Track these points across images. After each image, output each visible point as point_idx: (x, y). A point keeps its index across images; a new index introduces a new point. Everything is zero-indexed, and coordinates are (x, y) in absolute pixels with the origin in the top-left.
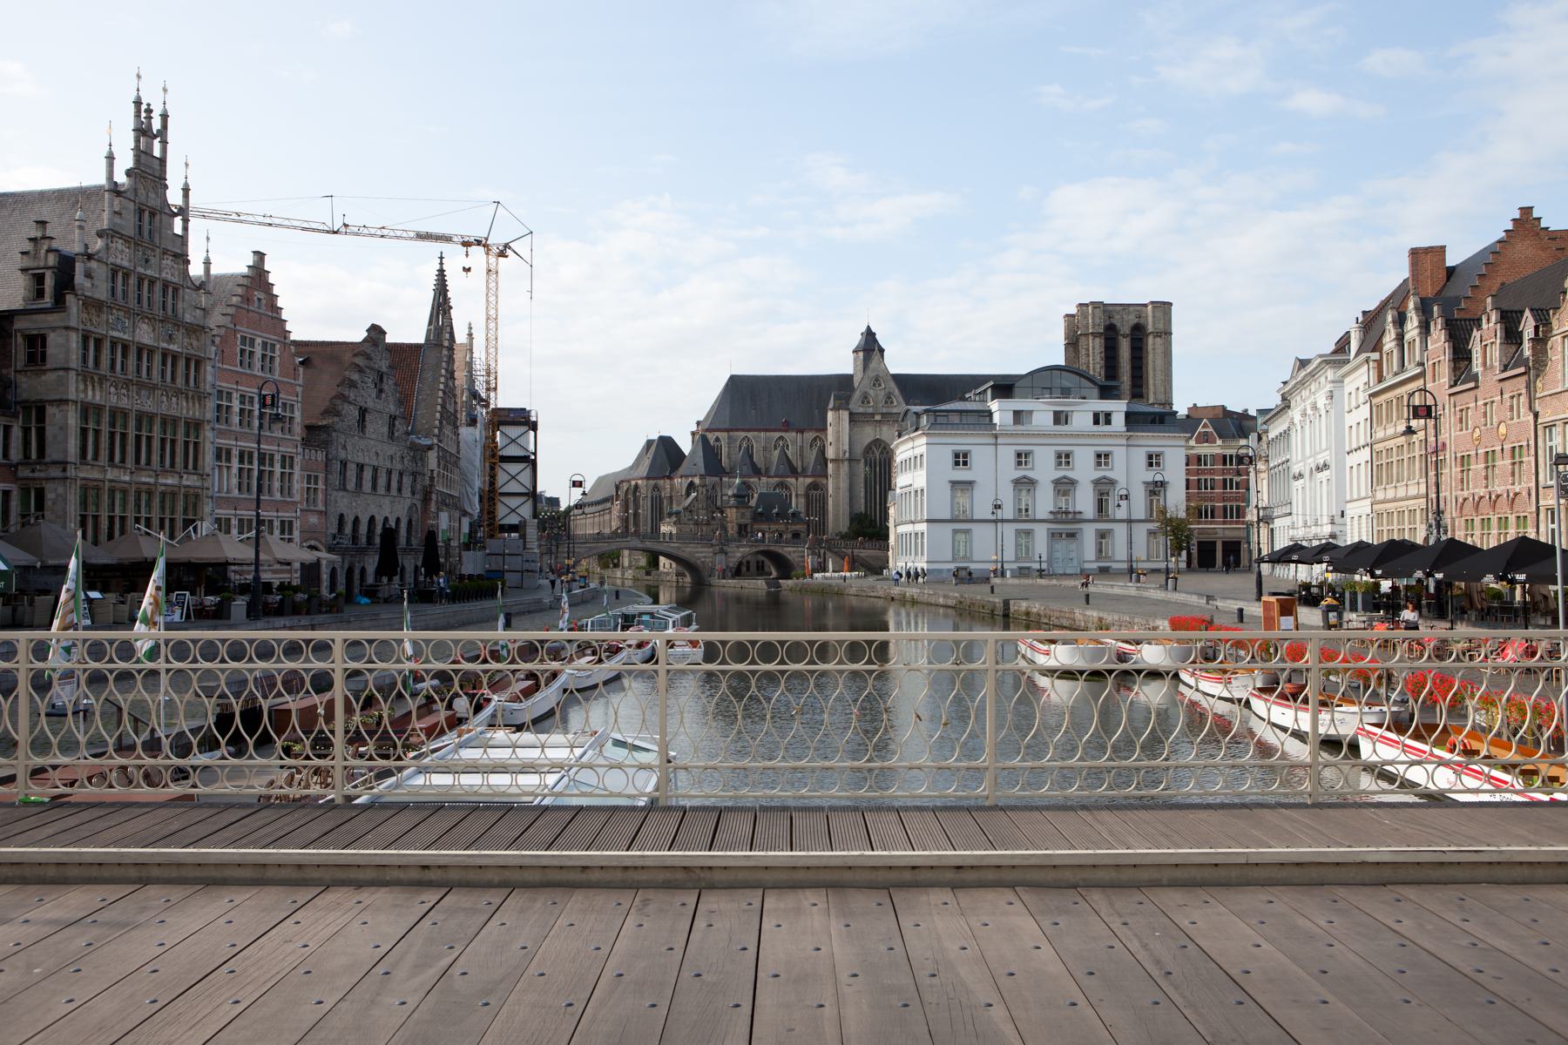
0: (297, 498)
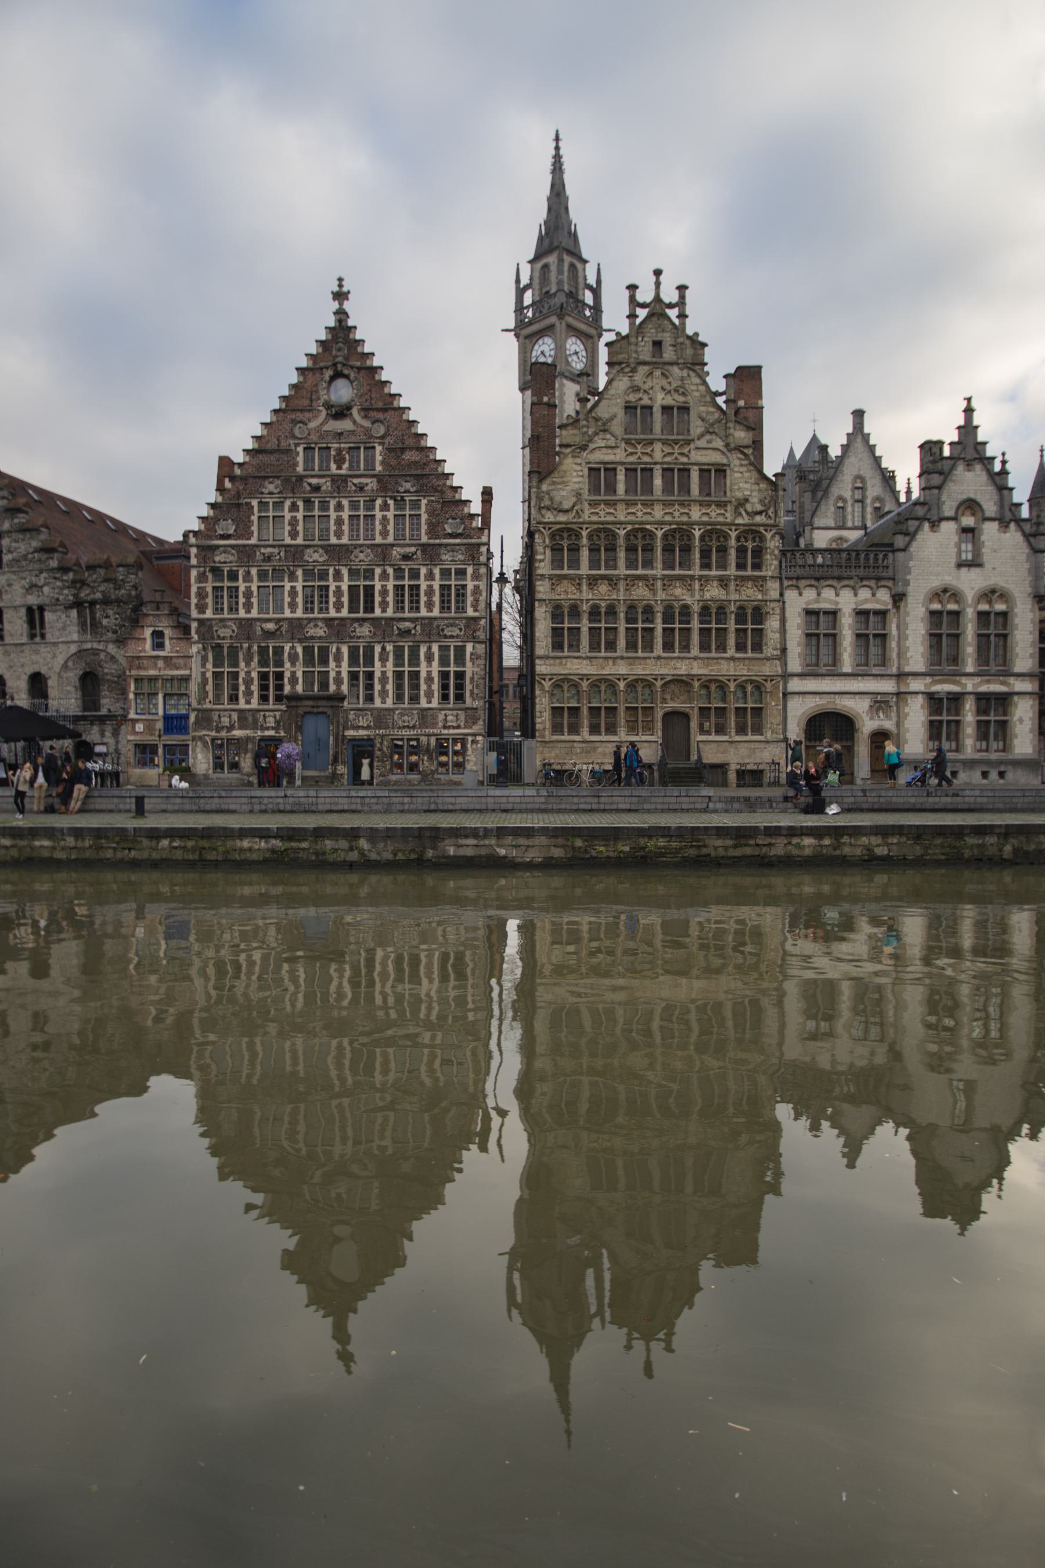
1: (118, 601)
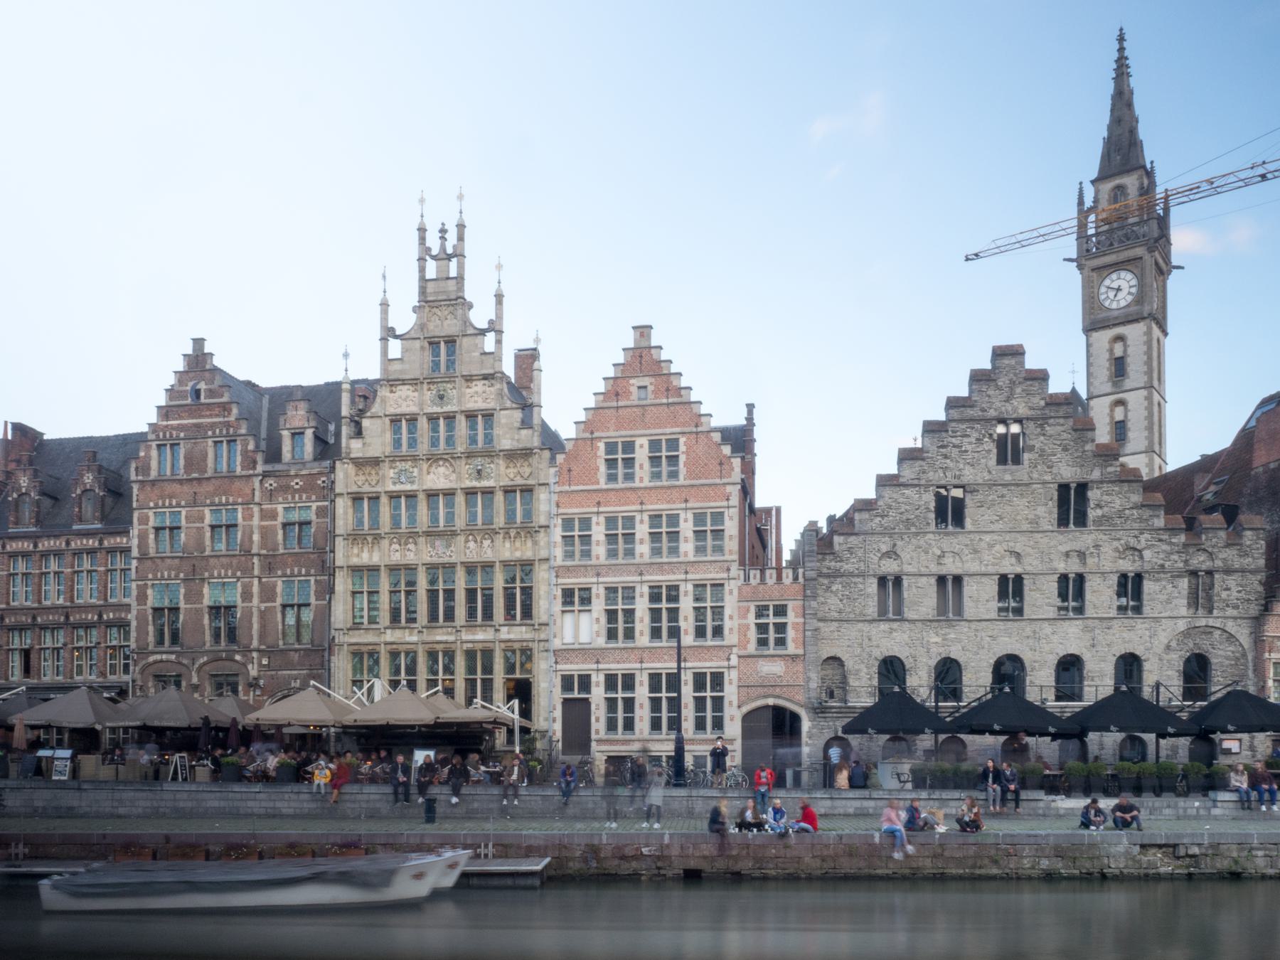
0: (730, 638)
1: (1243, 571)
